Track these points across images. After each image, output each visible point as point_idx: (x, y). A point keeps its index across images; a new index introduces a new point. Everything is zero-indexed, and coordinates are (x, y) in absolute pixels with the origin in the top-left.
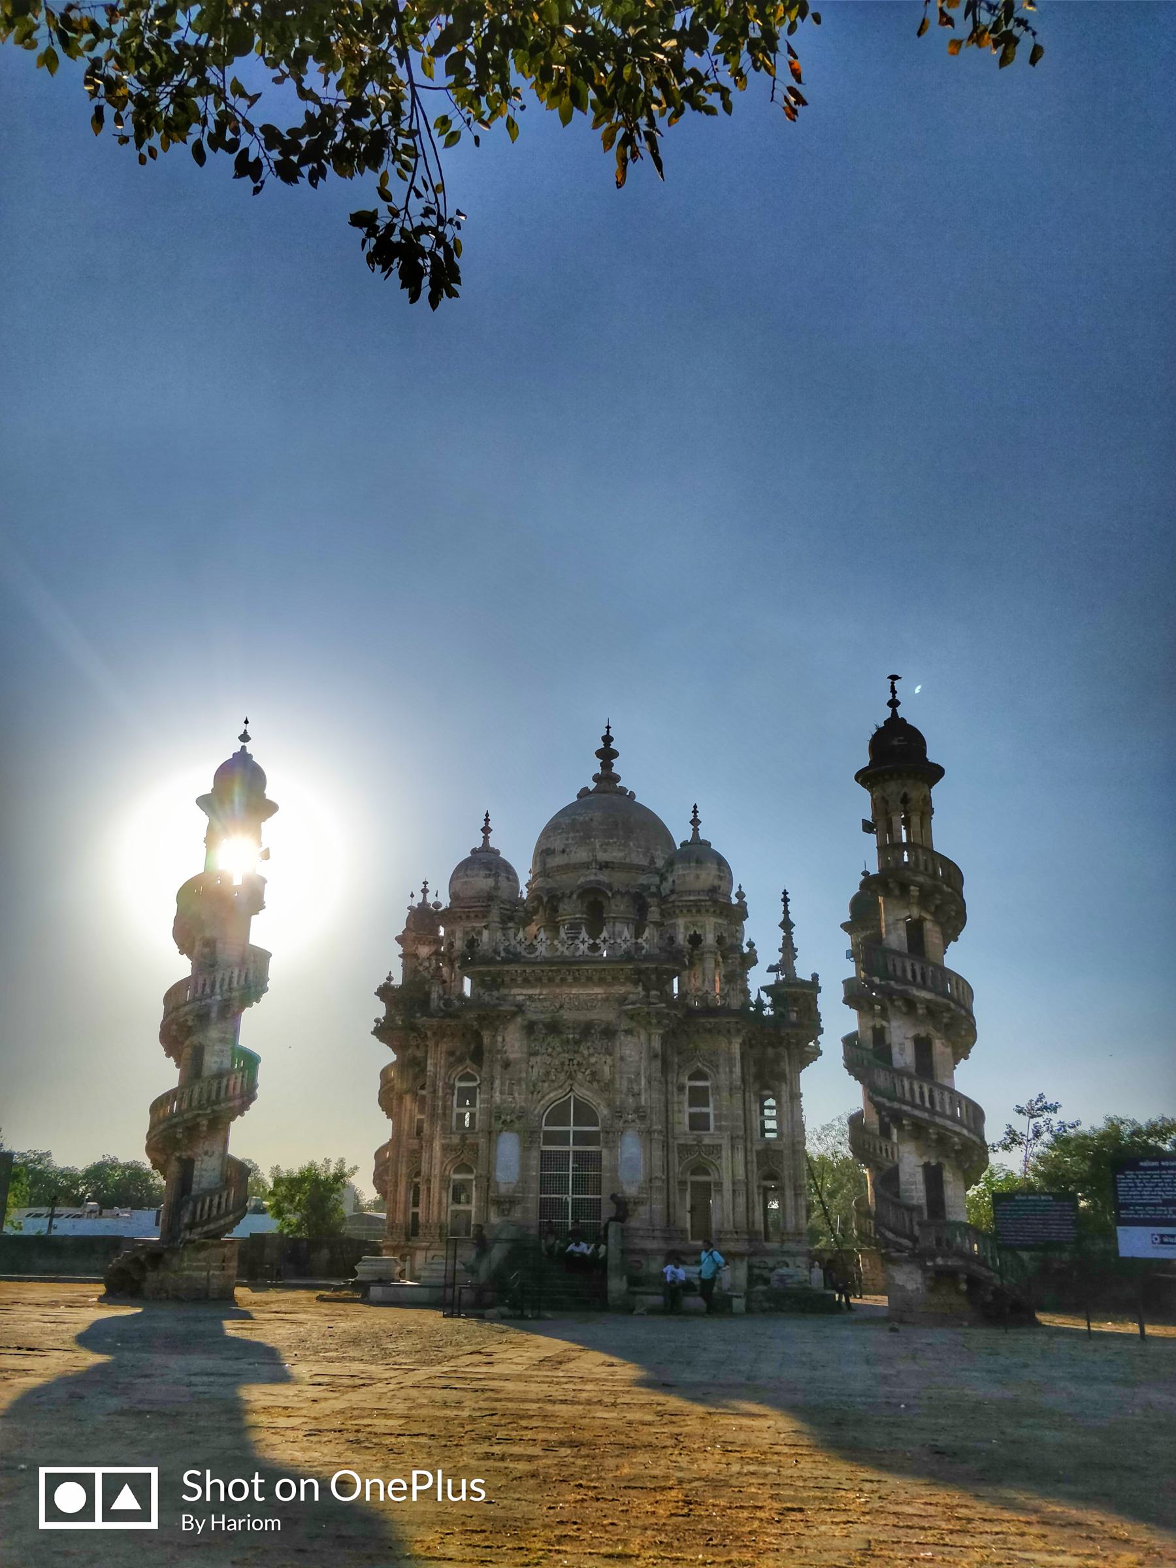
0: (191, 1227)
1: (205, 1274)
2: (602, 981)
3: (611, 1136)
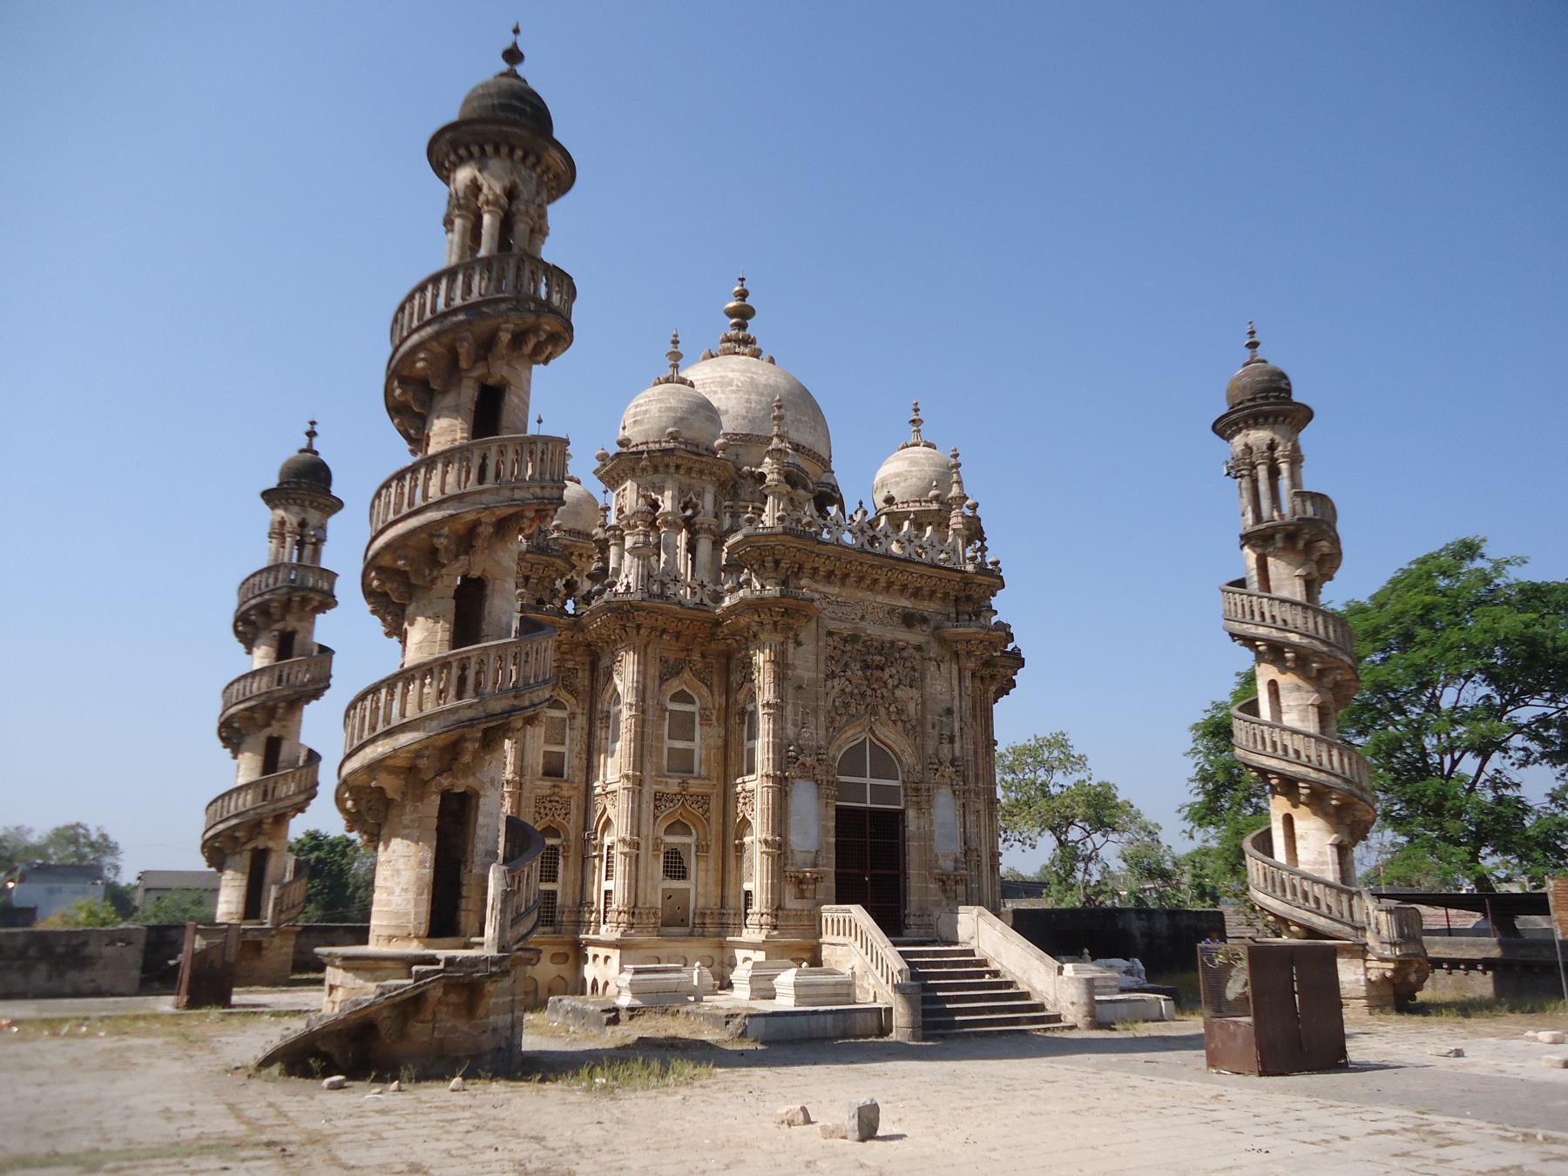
1: (509, 1017)
3: (920, 792)
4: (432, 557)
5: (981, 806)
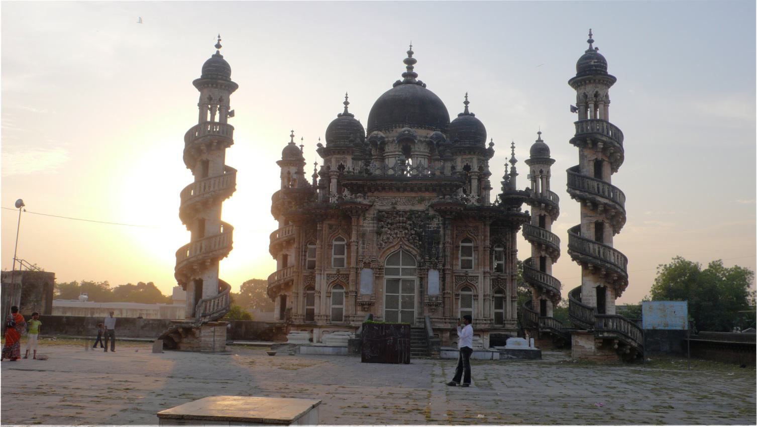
0: (204, 316)
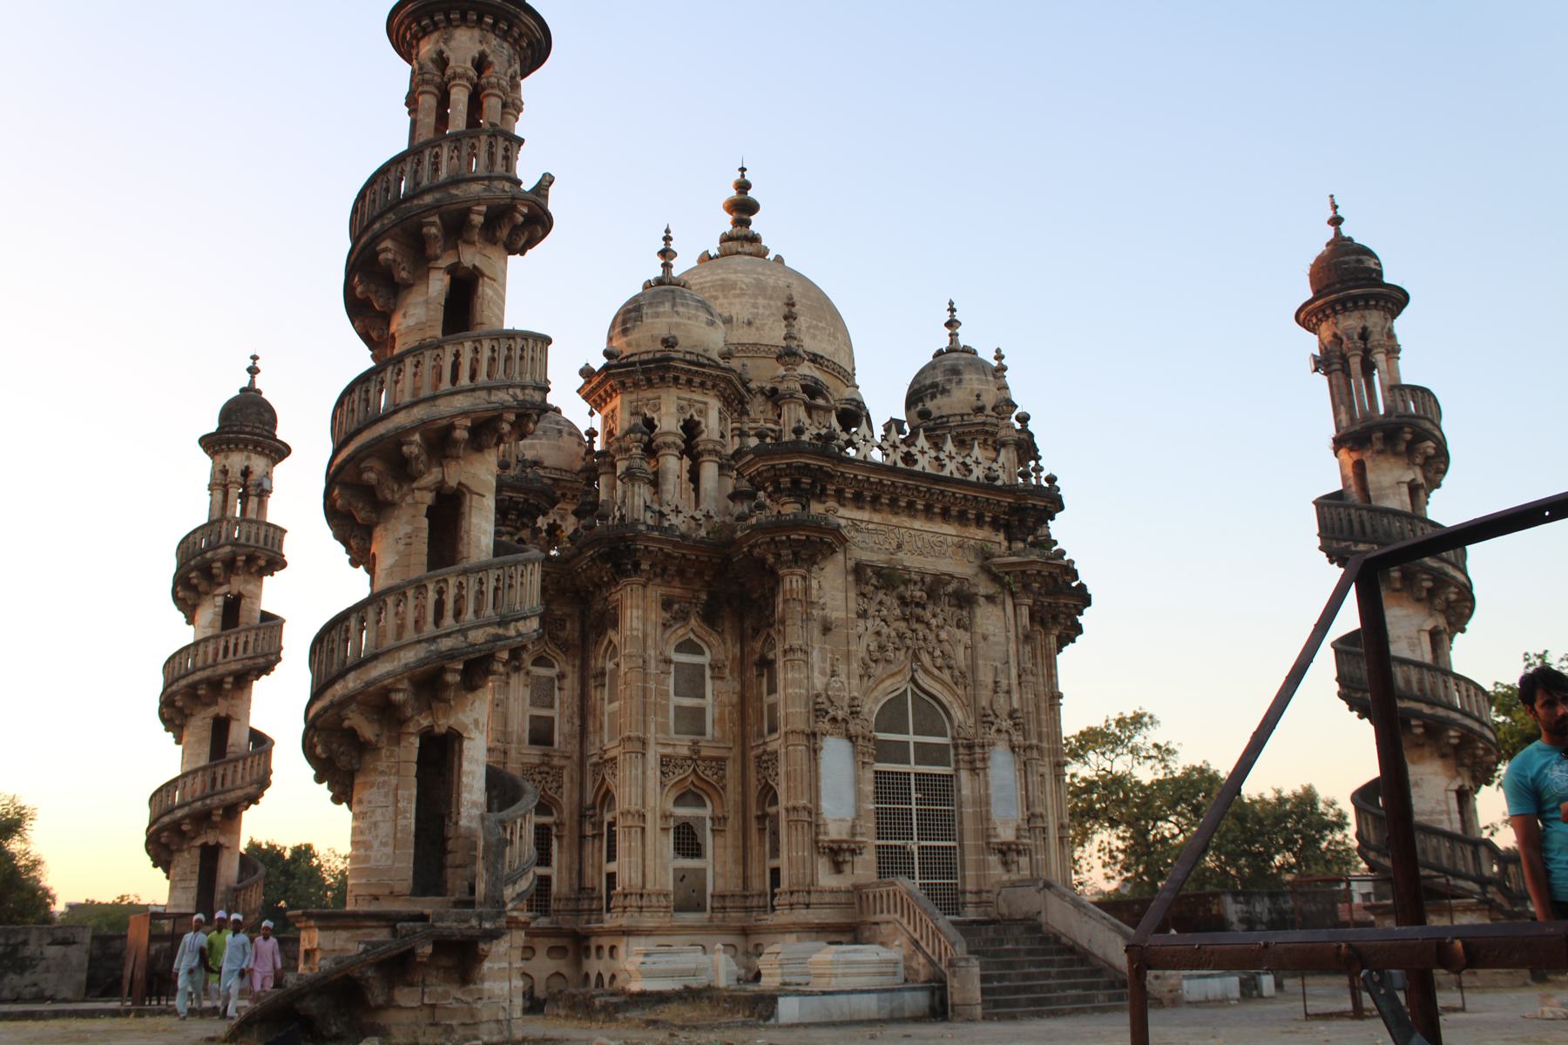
2: (962, 519)
3: (973, 754)
4: (403, 470)
5: (1046, 770)
